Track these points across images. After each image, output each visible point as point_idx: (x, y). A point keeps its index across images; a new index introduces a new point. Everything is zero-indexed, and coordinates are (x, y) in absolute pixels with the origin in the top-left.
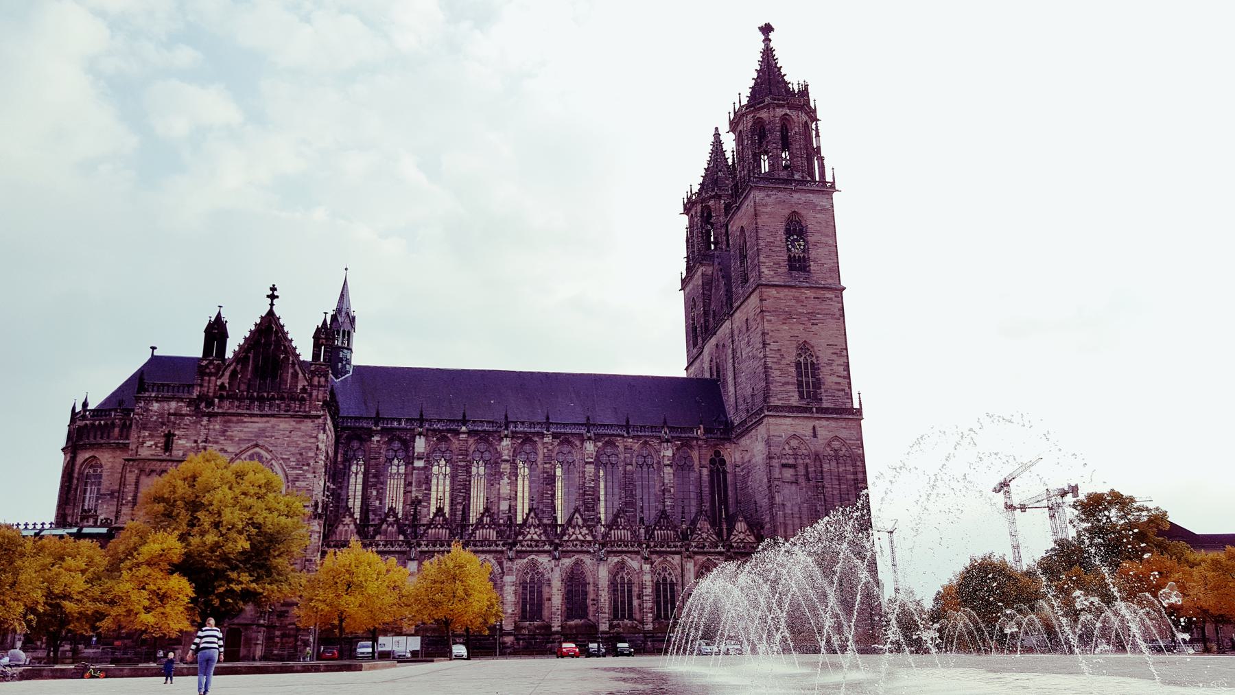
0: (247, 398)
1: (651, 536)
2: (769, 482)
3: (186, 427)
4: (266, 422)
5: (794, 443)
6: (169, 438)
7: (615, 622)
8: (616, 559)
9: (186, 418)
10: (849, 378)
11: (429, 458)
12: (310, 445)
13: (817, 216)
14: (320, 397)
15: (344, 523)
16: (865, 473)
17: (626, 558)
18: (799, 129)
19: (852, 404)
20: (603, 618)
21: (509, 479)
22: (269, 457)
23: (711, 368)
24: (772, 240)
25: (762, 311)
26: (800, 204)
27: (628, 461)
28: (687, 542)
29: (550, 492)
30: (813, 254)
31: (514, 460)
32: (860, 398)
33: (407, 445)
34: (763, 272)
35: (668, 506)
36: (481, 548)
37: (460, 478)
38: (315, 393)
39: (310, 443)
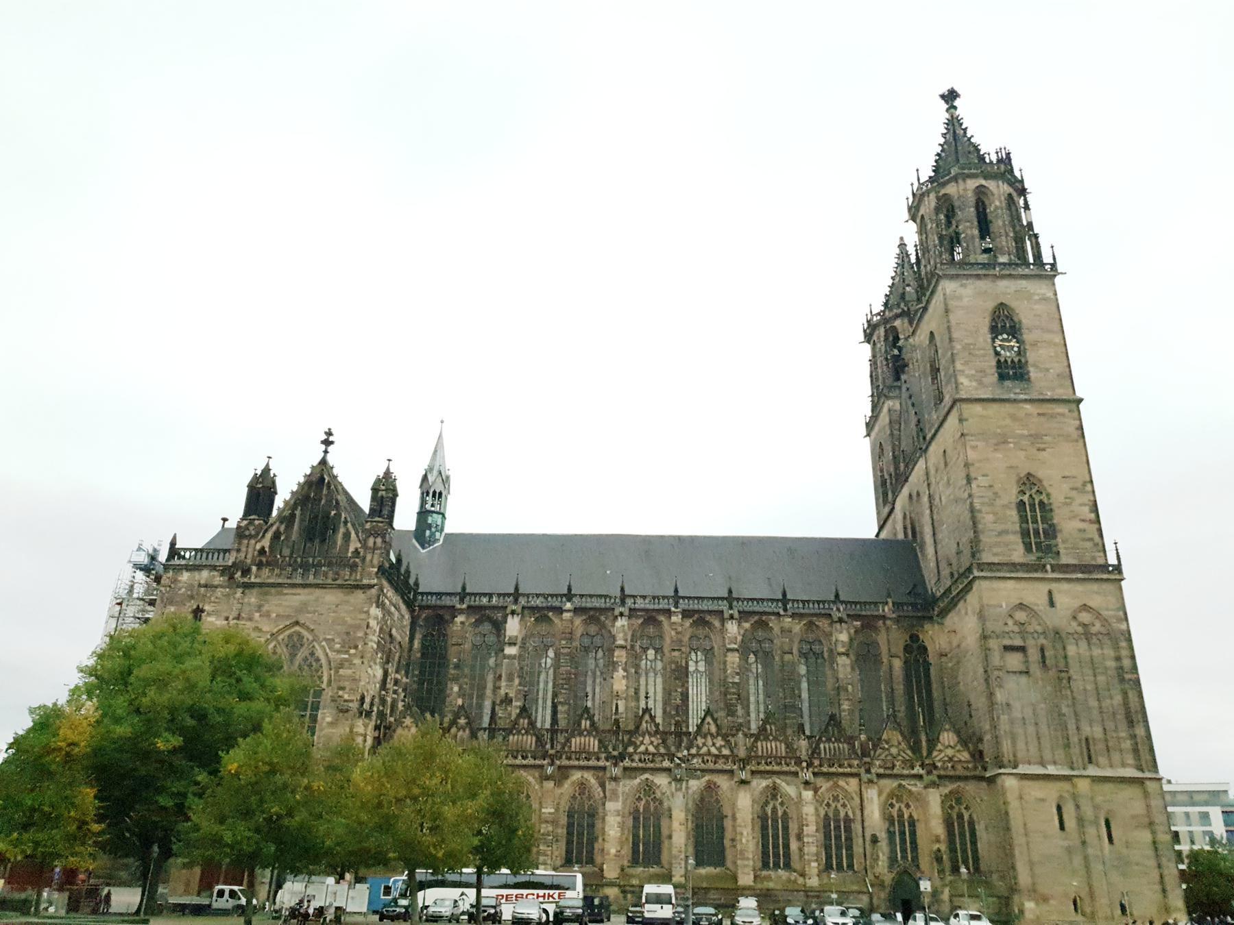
0: (290, 565)
2: (986, 671)
3: (217, 600)
4: (309, 594)
5: (1021, 616)
7: (764, 873)
8: (764, 783)
9: (218, 590)
10: (1098, 522)
11: (525, 644)
13: (1036, 307)
14: (375, 562)
15: (404, 725)
16: (1133, 657)
17: (778, 781)
19: (1106, 560)
20: (746, 866)
21: (625, 670)
22: (311, 638)
23: (905, 528)
24: (970, 341)
25: (962, 435)
27: (787, 648)
28: (867, 759)
30: (1031, 356)
31: (632, 647)
32: (1117, 550)
33: (499, 627)
34: (962, 384)
35: (844, 711)
36: (576, 763)
37: (563, 669)
38: (369, 557)
39: (360, 619)
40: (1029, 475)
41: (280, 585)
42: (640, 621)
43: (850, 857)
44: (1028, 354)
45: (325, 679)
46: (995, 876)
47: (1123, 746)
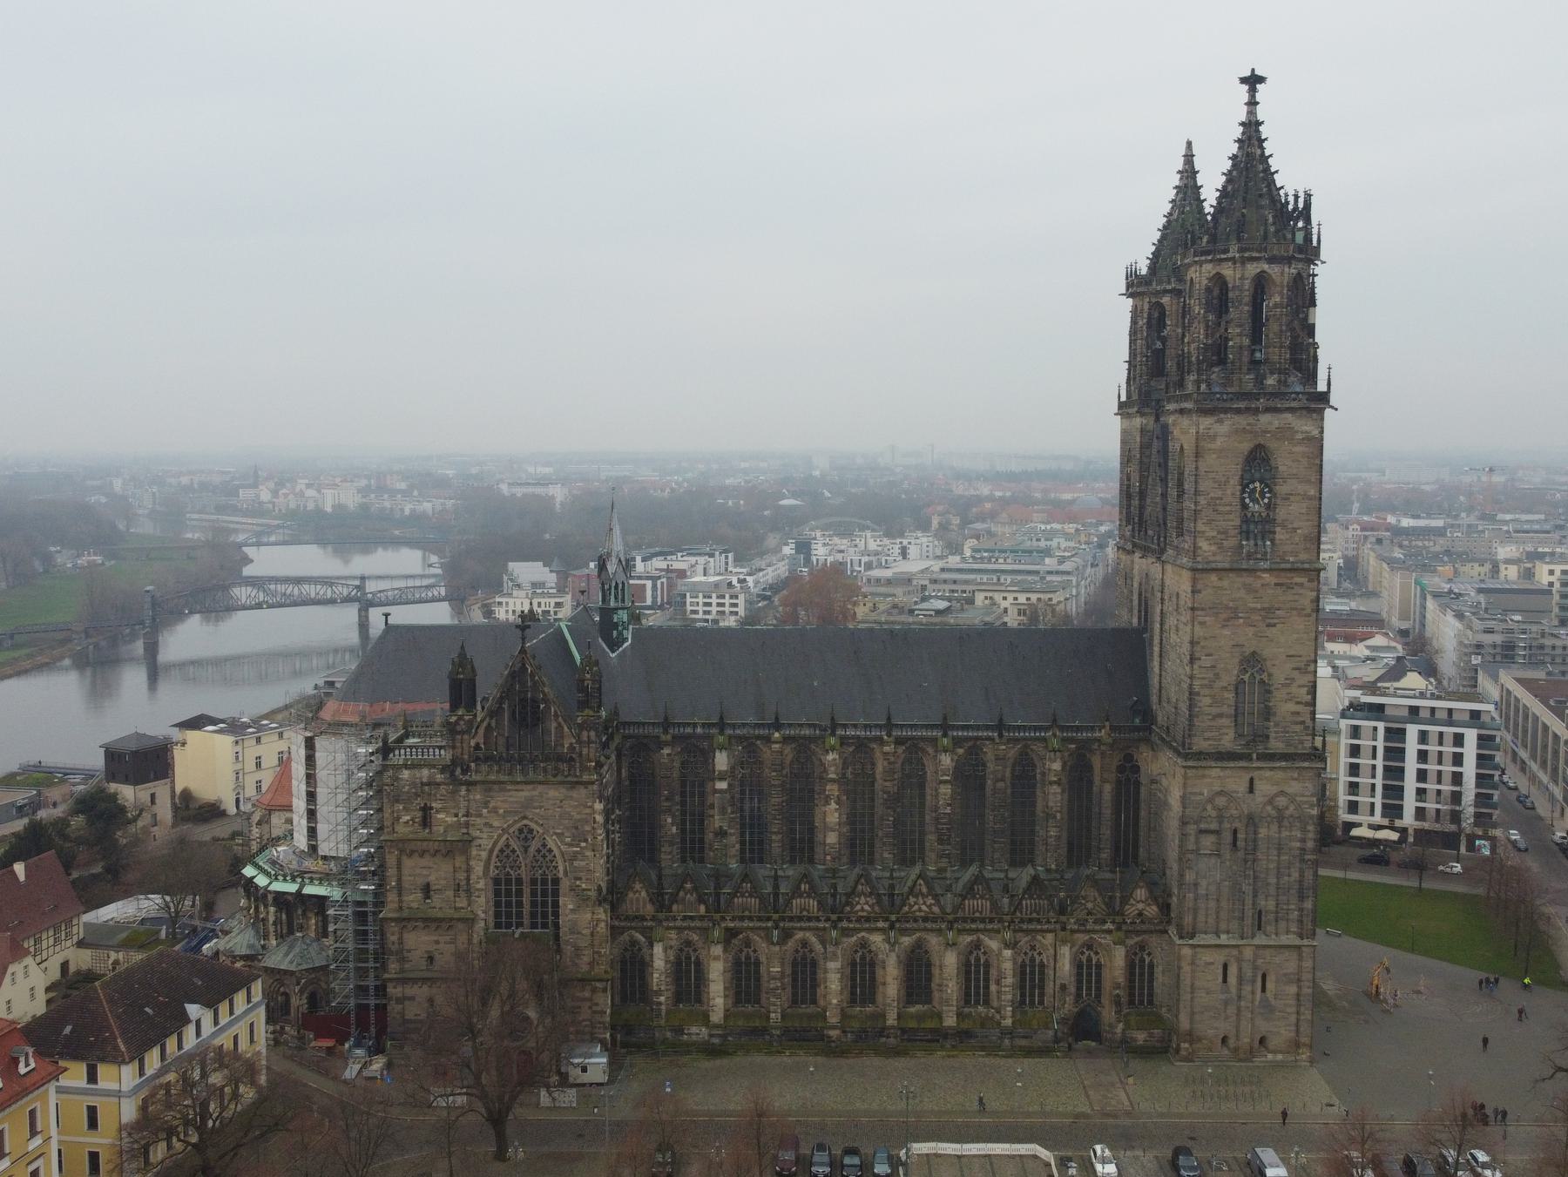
1: (1018, 907)
6: (426, 810)
7: (966, 1010)
8: (969, 939)
12: (584, 816)
17: (982, 937)
18: (1282, 298)
20: (950, 1011)
22: (541, 831)
26: (1269, 432)
29: (891, 819)
30: (1281, 513)
33: (707, 756)
34: (1200, 548)
38: (585, 751)
40: (1254, 653)
41: (503, 783)
42: (851, 750)
43: (1042, 995)
44: (1277, 511)
45: (561, 868)
46: (1164, 1009)
47: (1291, 917)
